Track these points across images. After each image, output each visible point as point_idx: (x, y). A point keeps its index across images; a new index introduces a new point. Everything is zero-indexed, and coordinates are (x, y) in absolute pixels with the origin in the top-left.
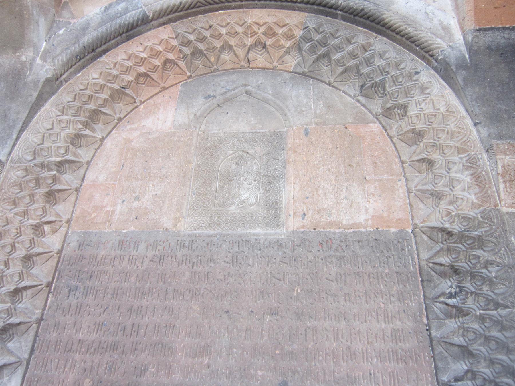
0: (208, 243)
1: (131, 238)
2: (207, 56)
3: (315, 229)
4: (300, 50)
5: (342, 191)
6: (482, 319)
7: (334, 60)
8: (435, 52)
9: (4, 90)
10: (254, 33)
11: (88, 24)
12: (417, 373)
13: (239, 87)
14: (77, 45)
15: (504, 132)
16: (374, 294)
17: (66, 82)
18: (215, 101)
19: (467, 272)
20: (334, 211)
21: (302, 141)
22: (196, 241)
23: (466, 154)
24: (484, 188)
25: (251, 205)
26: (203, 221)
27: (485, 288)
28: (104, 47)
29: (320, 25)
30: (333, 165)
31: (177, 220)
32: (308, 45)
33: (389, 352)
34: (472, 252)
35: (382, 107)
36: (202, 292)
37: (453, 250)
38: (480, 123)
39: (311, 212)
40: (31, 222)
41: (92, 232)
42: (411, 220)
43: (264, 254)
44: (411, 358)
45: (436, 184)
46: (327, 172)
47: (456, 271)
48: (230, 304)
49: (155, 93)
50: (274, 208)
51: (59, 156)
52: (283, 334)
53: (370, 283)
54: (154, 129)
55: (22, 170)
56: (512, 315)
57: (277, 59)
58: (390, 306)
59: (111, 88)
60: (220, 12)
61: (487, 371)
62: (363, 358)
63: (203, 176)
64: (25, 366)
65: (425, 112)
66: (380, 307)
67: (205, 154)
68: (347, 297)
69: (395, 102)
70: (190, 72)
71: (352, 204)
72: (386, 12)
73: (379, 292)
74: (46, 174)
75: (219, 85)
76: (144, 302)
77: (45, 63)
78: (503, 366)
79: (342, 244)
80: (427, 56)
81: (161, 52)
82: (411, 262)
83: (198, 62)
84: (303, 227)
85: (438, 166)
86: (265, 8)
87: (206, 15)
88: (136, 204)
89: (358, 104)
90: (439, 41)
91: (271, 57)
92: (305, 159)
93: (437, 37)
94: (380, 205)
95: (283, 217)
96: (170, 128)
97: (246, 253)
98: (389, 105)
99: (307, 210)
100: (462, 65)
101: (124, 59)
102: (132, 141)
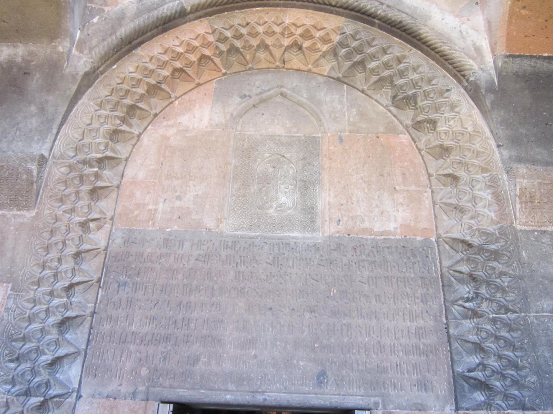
0: (250, 245)
1: (176, 237)
2: (244, 53)
3: (349, 235)
4: (335, 54)
5: (374, 199)
6: (494, 321)
7: (369, 68)
8: (466, 73)
9: (40, 81)
10: (292, 34)
11: (124, 14)
12: (436, 365)
13: (273, 88)
14: (114, 37)
15: (523, 155)
16: (401, 295)
17: (102, 74)
18: (251, 101)
19: (484, 281)
20: (366, 218)
21: (336, 148)
22: (239, 242)
23: (489, 174)
24: (503, 206)
25: (289, 209)
26: (244, 222)
27: (498, 295)
28: (140, 39)
29: (357, 33)
30: (365, 174)
31: (219, 221)
32: (344, 50)
33: (413, 347)
34: (489, 263)
35: (412, 119)
36: (246, 290)
37: (473, 261)
38: (503, 145)
39: (345, 219)
40: (78, 219)
41: (137, 230)
42: (435, 230)
43: (302, 257)
44: (432, 352)
45: (460, 199)
46: (360, 180)
47: (473, 278)
48: (273, 302)
49: (191, 88)
50: (310, 212)
51: (100, 153)
52: (321, 330)
53: (398, 286)
54: (191, 127)
55: (66, 166)
56: (519, 319)
57: (312, 61)
58: (415, 307)
59: (148, 83)
60: (257, 8)
61: (495, 364)
62: (391, 351)
63: (242, 177)
64: (83, 356)
65: (453, 130)
66: (406, 308)
67: (242, 155)
68: (378, 297)
69: (426, 117)
70: (225, 69)
71: (382, 212)
72: (423, 27)
73: (405, 294)
74: (88, 170)
75: (254, 85)
76: (192, 298)
77: (81, 55)
78: (509, 361)
79: (374, 250)
80: (458, 74)
81: (197, 47)
82: (434, 268)
83: (233, 58)
84: (338, 232)
85: (463, 182)
86: (303, 8)
87: (243, 10)
88: (178, 203)
89: (390, 114)
90: (471, 62)
91: (306, 60)
92: (339, 166)
93: (470, 58)
94: (408, 214)
95: (319, 222)
96: (207, 127)
97: (286, 255)
98: (419, 119)
99: (342, 217)
100: (491, 89)
101: (160, 53)
102: (168, 138)
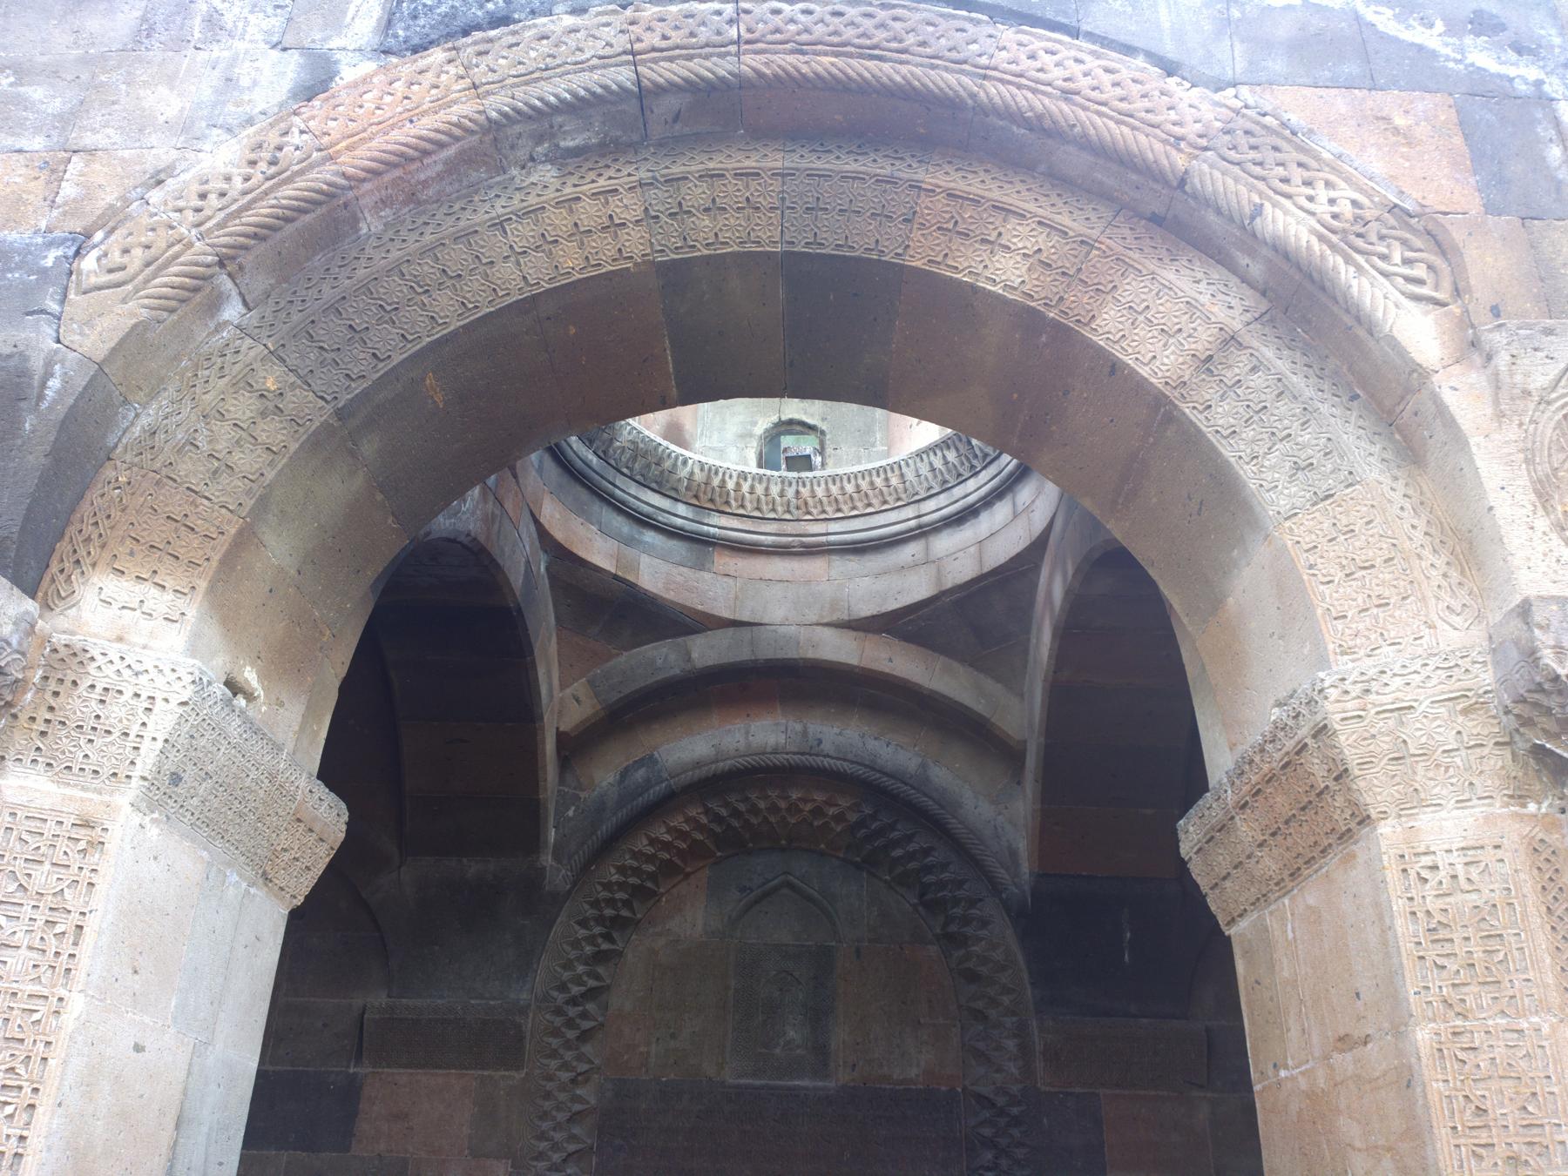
25: (798, 1047)
74: (572, 1012)
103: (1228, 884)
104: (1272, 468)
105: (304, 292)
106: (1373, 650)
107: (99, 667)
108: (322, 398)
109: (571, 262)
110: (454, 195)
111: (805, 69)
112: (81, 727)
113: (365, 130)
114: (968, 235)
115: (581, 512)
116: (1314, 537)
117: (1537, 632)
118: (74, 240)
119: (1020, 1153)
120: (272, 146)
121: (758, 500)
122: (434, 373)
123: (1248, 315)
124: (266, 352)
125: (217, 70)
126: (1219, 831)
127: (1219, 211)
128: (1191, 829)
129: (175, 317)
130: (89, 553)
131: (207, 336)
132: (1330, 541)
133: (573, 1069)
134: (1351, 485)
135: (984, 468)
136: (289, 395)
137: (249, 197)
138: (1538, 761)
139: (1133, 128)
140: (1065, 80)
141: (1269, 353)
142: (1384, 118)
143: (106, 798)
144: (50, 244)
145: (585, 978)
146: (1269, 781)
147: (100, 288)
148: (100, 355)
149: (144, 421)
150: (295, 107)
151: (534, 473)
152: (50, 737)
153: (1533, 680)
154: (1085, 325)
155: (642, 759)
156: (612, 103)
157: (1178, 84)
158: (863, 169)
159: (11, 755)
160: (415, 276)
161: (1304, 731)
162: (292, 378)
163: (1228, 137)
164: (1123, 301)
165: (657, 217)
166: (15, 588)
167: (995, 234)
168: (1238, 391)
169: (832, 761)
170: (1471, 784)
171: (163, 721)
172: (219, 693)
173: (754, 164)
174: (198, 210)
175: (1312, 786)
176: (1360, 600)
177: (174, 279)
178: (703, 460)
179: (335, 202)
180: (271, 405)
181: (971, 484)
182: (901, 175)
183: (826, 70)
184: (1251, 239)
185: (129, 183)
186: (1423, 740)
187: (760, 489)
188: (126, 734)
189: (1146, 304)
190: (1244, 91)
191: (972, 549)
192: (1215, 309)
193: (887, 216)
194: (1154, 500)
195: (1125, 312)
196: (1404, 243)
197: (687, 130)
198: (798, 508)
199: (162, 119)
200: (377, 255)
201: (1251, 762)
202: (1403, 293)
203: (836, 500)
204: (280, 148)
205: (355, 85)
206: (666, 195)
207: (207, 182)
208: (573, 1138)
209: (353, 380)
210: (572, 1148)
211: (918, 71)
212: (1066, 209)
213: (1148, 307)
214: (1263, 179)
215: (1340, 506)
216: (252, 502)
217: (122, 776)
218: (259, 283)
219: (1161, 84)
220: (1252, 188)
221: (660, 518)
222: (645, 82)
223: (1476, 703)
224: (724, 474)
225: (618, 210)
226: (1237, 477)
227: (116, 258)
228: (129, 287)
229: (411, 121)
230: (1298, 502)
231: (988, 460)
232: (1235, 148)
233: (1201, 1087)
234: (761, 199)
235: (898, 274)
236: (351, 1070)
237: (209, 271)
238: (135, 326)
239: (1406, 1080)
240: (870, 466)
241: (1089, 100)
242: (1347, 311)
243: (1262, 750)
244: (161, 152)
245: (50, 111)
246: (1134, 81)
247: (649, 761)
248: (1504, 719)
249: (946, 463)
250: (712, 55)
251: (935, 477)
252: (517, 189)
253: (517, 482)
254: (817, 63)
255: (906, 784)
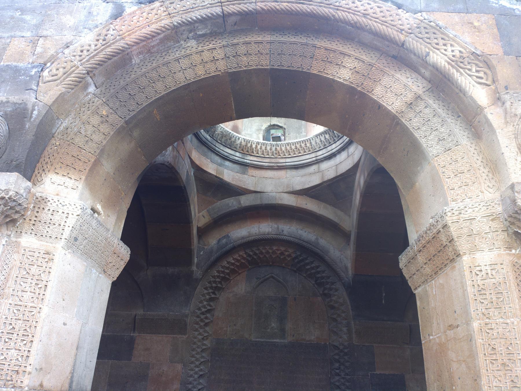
25: (275, 329)
74: (202, 317)
84: (293, 340)
103: (415, 276)
104: (431, 140)
105: (115, 83)
106: (463, 200)
107: (51, 204)
108: (121, 117)
109: (201, 72)
110: (163, 50)
111: (278, 7)
112: (46, 222)
113: (134, 29)
114: (331, 62)
115: (205, 155)
116: (444, 163)
117: (516, 194)
118: (41, 66)
119: (347, 364)
120: (104, 35)
121: (263, 151)
122: (156, 109)
123: (424, 89)
124: (103, 102)
125: (86, 10)
126: (412, 259)
127: (415, 54)
128: (403, 259)
129: (73, 91)
130: (47, 167)
131: (84, 97)
132: (450, 164)
133: (203, 335)
134: (457, 146)
135: (338, 140)
136: (110, 116)
137: (97, 51)
138: (516, 236)
139: (387, 26)
140: (364, 10)
141: (431, 102)
142: (470, 23)
143: (54, 245)
144: (33, 67)
145: (207, 306)
146: (428, 243)
147: (49, 82)
148: (50, 103)
149: (64, 125)
150: (111, 22)
151: (189, 142)
152: (36, 225)
153: (514, 210)
154: (370, 92)
155: (225, 236)
156: (215, 19)
157: (402, 12)
158: (297, 40)
159: (24, 231)
160: (150, 77)
161: (440, 226)
162: (111, 111)
163: (418, 30)
164: (383, 84)
165: (229, 57)
166: (24, 178)
167: (340, 62)
168: (420, 114)
169: (287, 237)
170: (494, 244)
171: (72, 221)
172: (89, 212)
173: (261, 39)
174: (80, 56)
175: (442, 244)
176: (459, 184)
177: (73, 78)
178: (245, 138)
179: (124, 53)
180: (104, 120)
181: (334, 146)
182: (309, 42)
183: (285, 7)
184: (425, 63)
185: (58, 47)
186: (478, 229)
187: (263, 148)
188: (60, 225)
189: (390, 85)
190: (424, 14)
191: (334, 168)
192: (413, 87)
193: (305, 56)
194: (393, 151)
195: (383, 88)
196: (477, 65)
197: (239, 28)
198: (276, 154)
199: (68, 26)
200: (138, 70)
201: (423, 236)
202: (475, 82)
203: (289, 151)
204: (106, 35)
205: (130, 14)
206: (232, 50)
207: (83, 47)
208: (203, 357)
209: (130, 111)
210: (202, 360)
211: (315, 8)
212: (364, 53)
213: (391, 86)
214: (430, 43)
215: (453, 152)
216: (99, 151)
217: (59, 238)
218: (100, 79)
219: (396, 12)
220: (426, 47)
221: (231, 157)
222: (225, 12)
223: (496, 217)
224: (252, 143)
225: (216, 55)
226: (420, 143)
227: (54, 72)
228: (59, 81)
229: (149, 26)
230: (440, 151)
231: (340, 138)
232: (420, 33)
233: (407, 344)
234: (263, 51)
235: (308, 76)
236: (132, 335)
237: (84, 76)
238: (61, 94)
239: (470, 339)
240: (300, 140)
241: (372, 17)
242: (457, 88)
243: (426, 233)
244: (68, 37)
245: (32, 23)
246: (387, 11)
247: (227, 236)
248: (505, 222)
249: (326, 139)
250: (247, 3)
251: (322, 143)
252: (183, 48)
253: (184, 146)
254: (282, 5)
255: (311, 245)
